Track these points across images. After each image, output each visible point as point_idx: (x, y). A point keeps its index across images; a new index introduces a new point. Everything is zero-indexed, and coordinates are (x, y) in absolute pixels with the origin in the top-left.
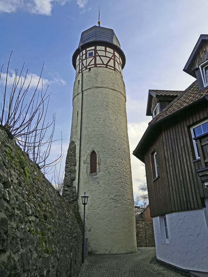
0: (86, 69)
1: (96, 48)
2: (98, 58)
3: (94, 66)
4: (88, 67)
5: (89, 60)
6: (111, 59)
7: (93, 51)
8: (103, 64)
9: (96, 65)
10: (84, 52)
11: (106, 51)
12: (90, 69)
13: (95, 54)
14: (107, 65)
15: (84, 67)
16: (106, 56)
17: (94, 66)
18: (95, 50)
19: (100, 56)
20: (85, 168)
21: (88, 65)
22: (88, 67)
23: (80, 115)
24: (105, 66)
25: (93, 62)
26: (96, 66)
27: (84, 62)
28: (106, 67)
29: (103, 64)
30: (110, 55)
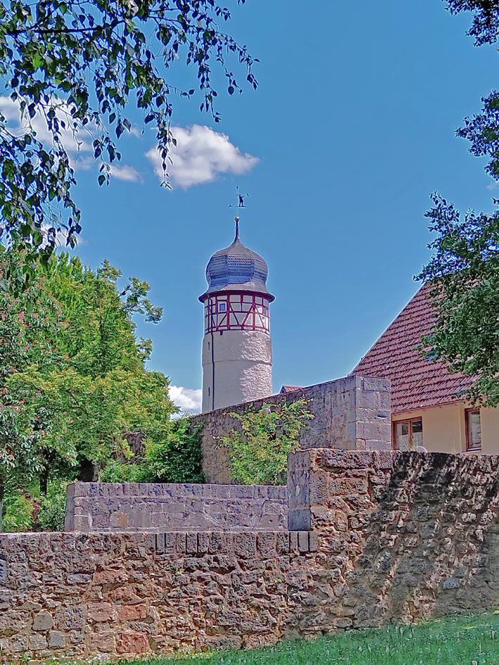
1: (228, 298)
4: (219, 329)
5: (221, 316)
6: (249, 313)
7: (226, 303)
8: (238, 325)
9: (228, 326)
10: (214, 299)
13: (228, 309)
14: (243, 325)
16: (242, 312)
18: (228, 301)
19: (234, 312)
21: (220, 326)
22: (219, 329)
23: (211, 393)
24: (240, 328)
25: (225, 323)
27: (215, 316)
28: (243, 329)
29: (238, 325)
30: (247, 307)
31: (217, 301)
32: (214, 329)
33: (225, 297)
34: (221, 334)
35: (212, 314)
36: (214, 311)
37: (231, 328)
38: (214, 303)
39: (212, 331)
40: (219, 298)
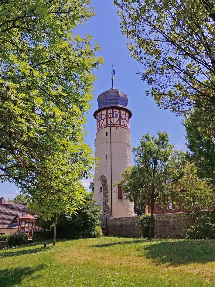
0: (114, 126)
2: (121, 120)
3: (119, 126)
4: (115, 125)
7: (118, 113)
8: (124, 126)
9: (120, 126)
10: (111, 110)
11: (125, 115)
12: (117, 127)
15: (112, 124)
17: (119, 126)
18: (120, 112)
19: (123, 119)
20: (115, 195)
22: (115, 125)
25: (118, 123)
26: (120, 127)
27: (112, 119)
29: (124, 126)
31: (113, 112)
32: (113, 126)
33: (118, 111)
34: (117, 128)
35: (110, 118)
36: (112, 116)
37: (122, 126)
38: (112, 112)
39: (111, 127)
40: (114, 110)
